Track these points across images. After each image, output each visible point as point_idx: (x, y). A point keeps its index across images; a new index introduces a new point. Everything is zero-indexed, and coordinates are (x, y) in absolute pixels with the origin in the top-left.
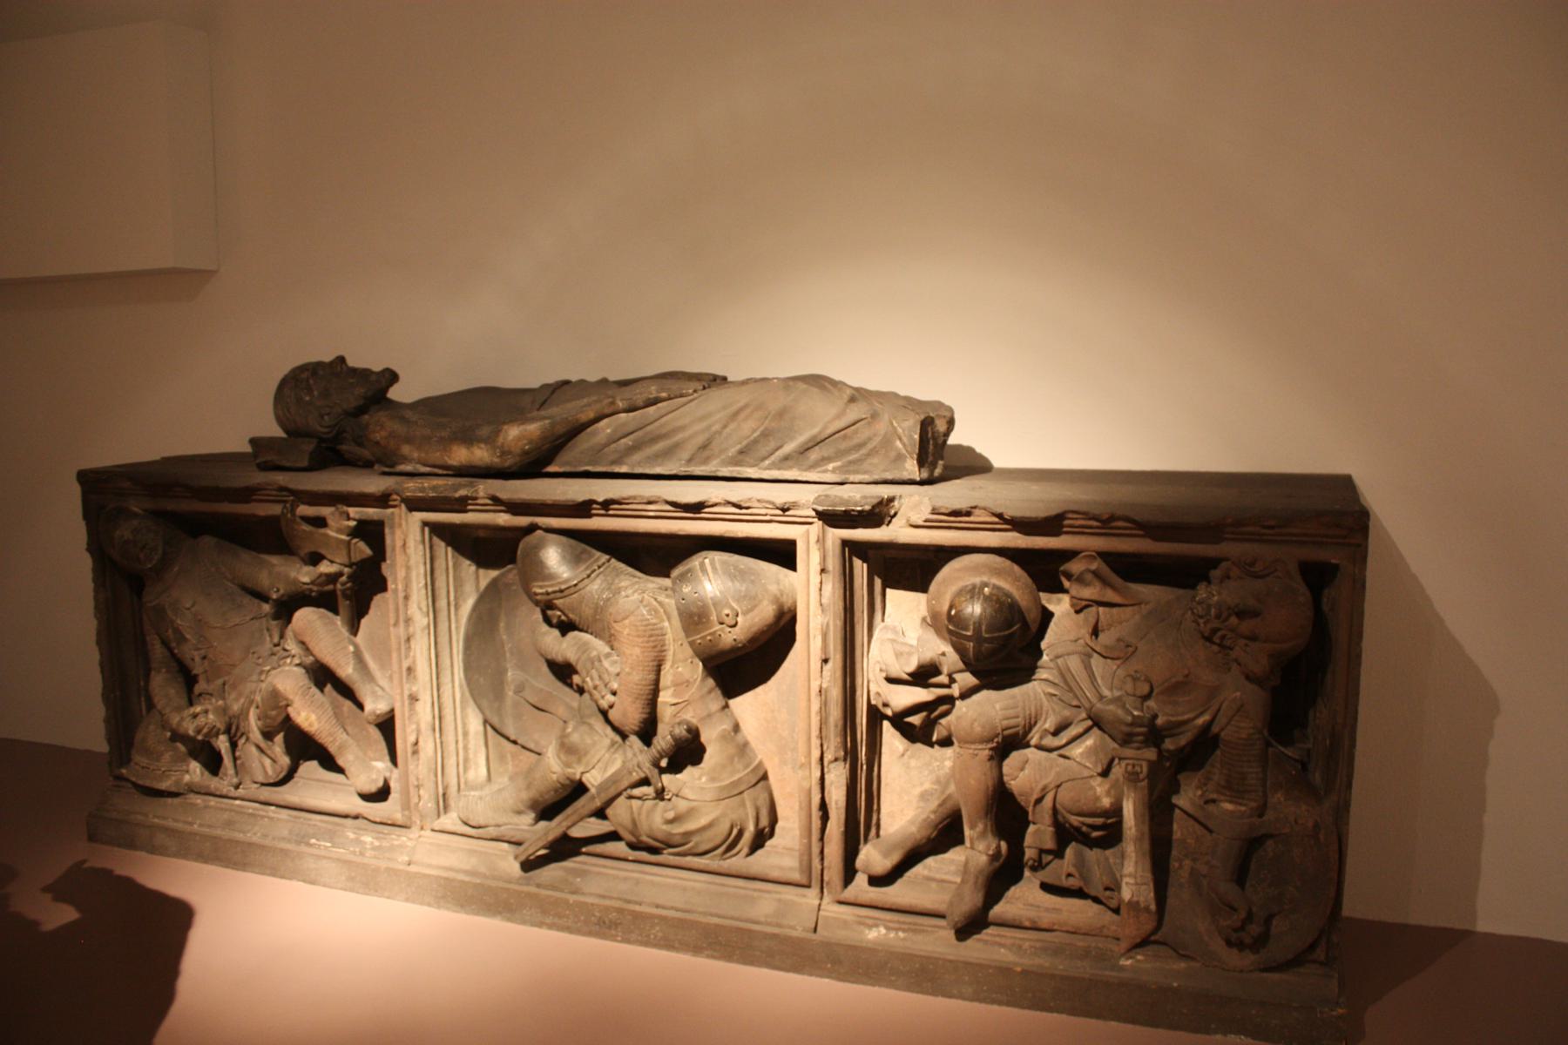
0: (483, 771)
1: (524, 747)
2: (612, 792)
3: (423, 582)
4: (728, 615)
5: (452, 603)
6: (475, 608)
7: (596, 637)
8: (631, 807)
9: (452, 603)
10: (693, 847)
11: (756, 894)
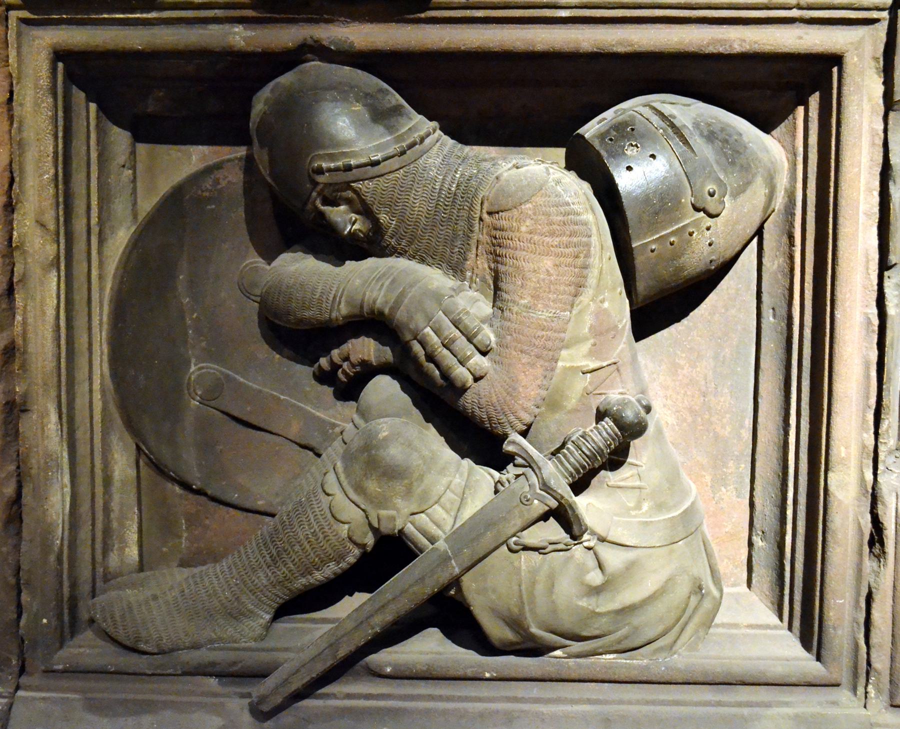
0: (133, 553)
1: (214, 499)
2: (488, 540)
3: (52, 171)
4: (712, 195)
5: (95, 230)
6: (136, 243)
7: (422, 261)
8: (518, 570)
9: (95, 230)
10: (626, 637)
11: (746, 711)
